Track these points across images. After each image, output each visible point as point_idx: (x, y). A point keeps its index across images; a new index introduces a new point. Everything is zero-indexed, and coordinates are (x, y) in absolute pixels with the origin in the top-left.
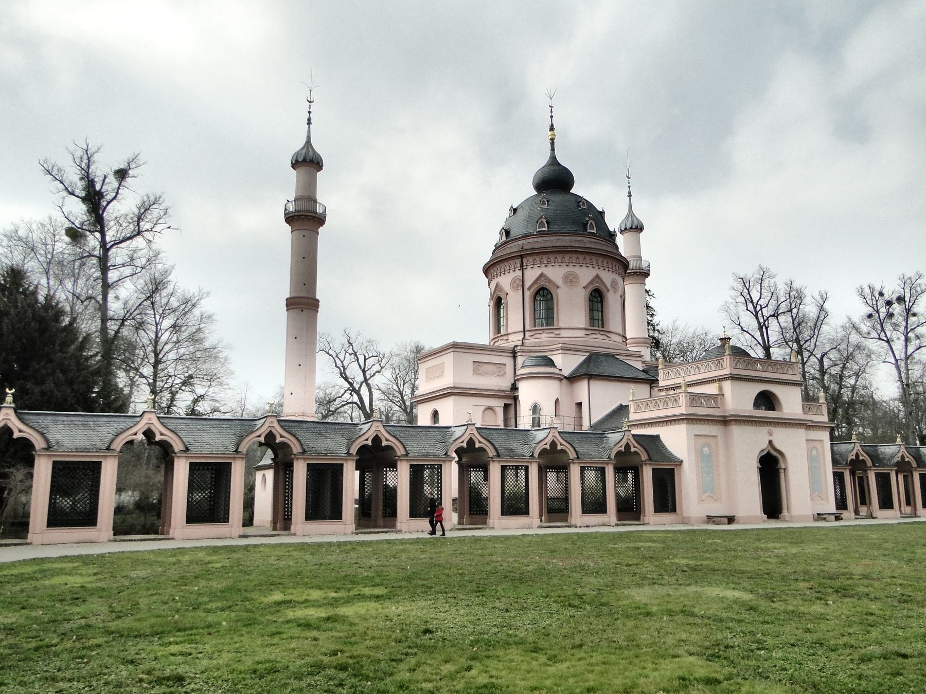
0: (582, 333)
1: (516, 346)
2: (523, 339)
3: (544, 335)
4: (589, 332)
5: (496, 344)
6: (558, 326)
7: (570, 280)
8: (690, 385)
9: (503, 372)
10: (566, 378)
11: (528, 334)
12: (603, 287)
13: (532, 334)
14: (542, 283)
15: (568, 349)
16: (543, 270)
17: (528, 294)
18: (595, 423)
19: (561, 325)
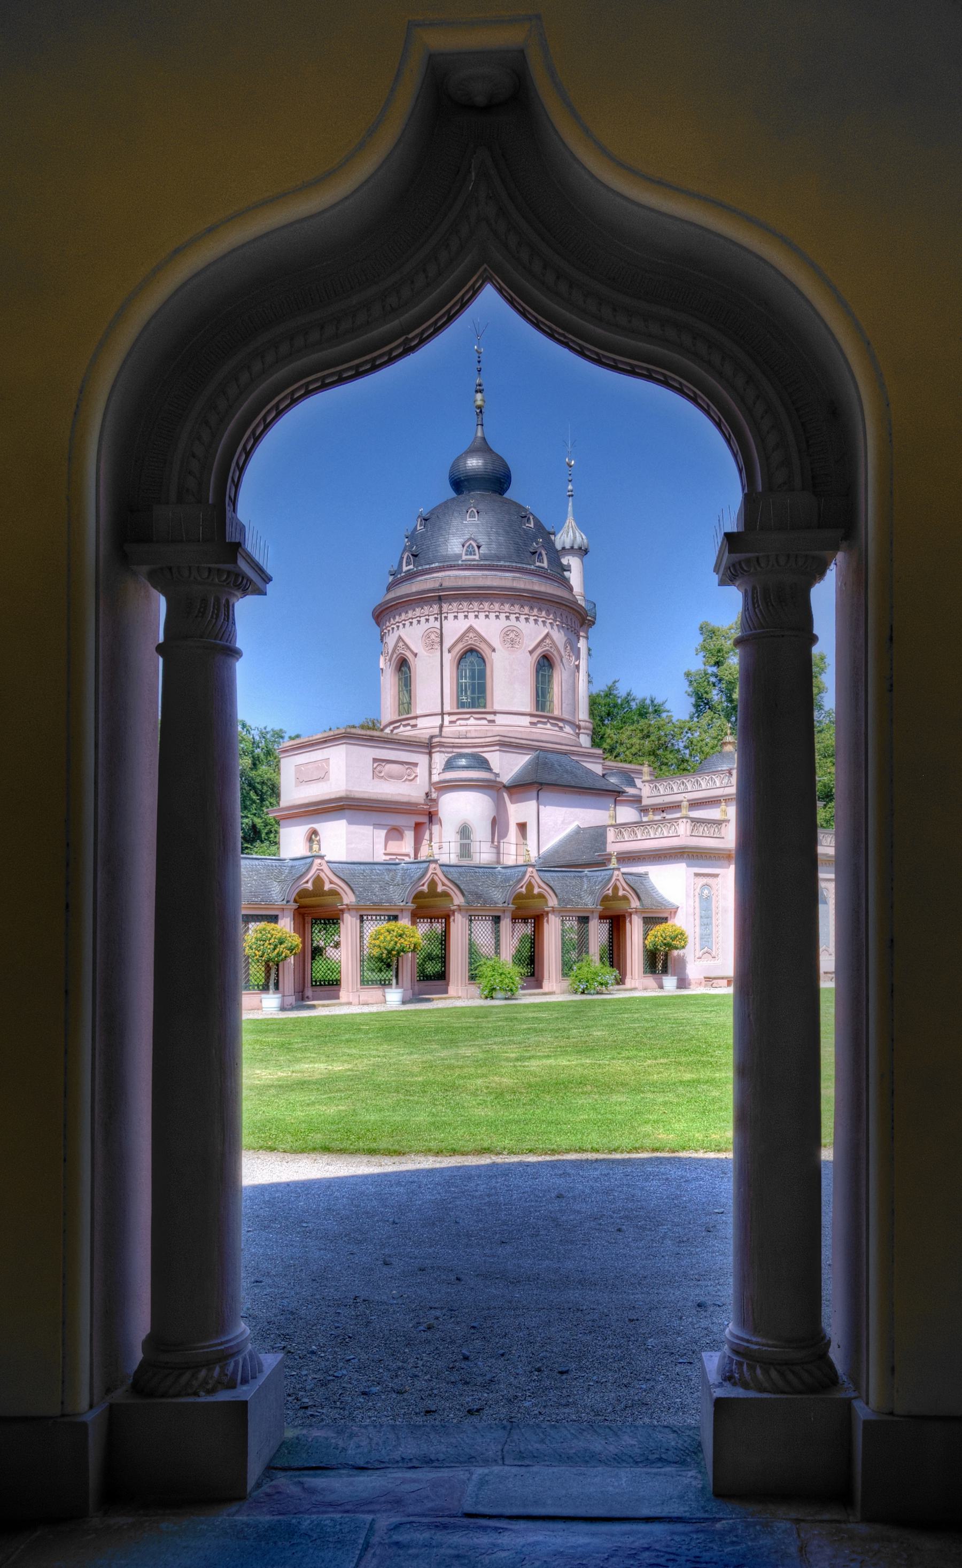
0: (526, 721)
1: (432, 737)
2: (442, 726)
3: (472, 721)
4: (535, 720)
5: (395, 731)
6: (493, 708)
7: (511, 639)
8: (696, 804)
9: (414, 775)
10: (504, 786)
11: (447, 718)
12: (555, 653)
13: (454, 718)
14: (471, 641)
15: (507, 745)
16: (472, 621)
17: (447, 657)
18: (548, 851)
19: (497, 707)
